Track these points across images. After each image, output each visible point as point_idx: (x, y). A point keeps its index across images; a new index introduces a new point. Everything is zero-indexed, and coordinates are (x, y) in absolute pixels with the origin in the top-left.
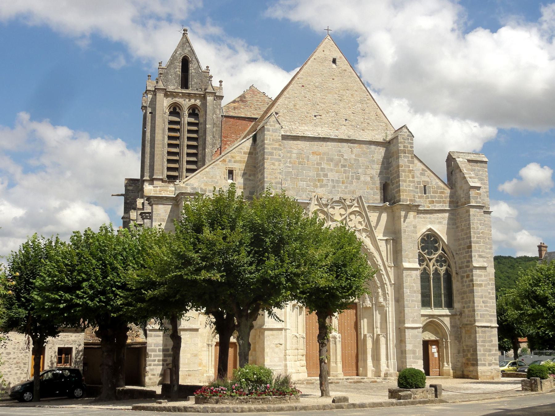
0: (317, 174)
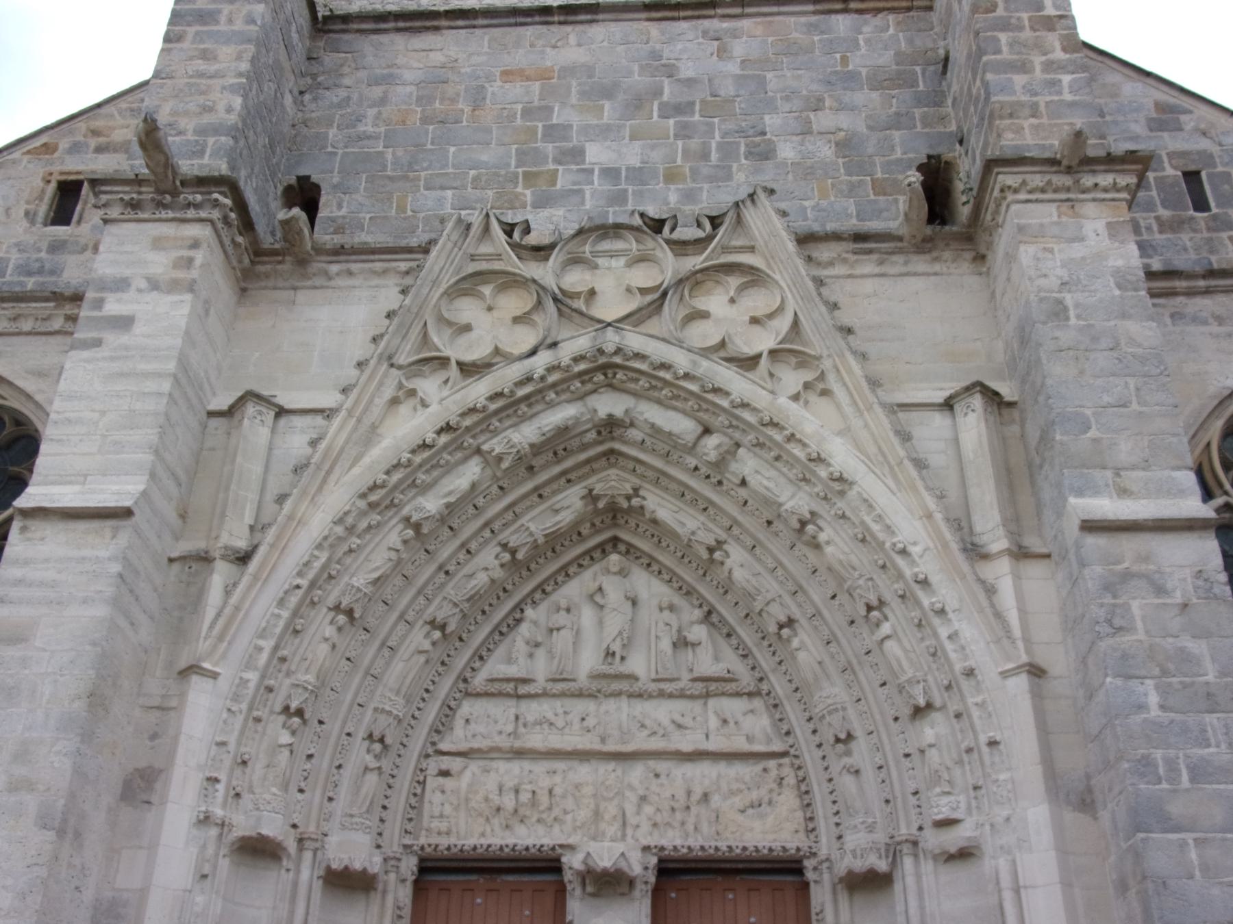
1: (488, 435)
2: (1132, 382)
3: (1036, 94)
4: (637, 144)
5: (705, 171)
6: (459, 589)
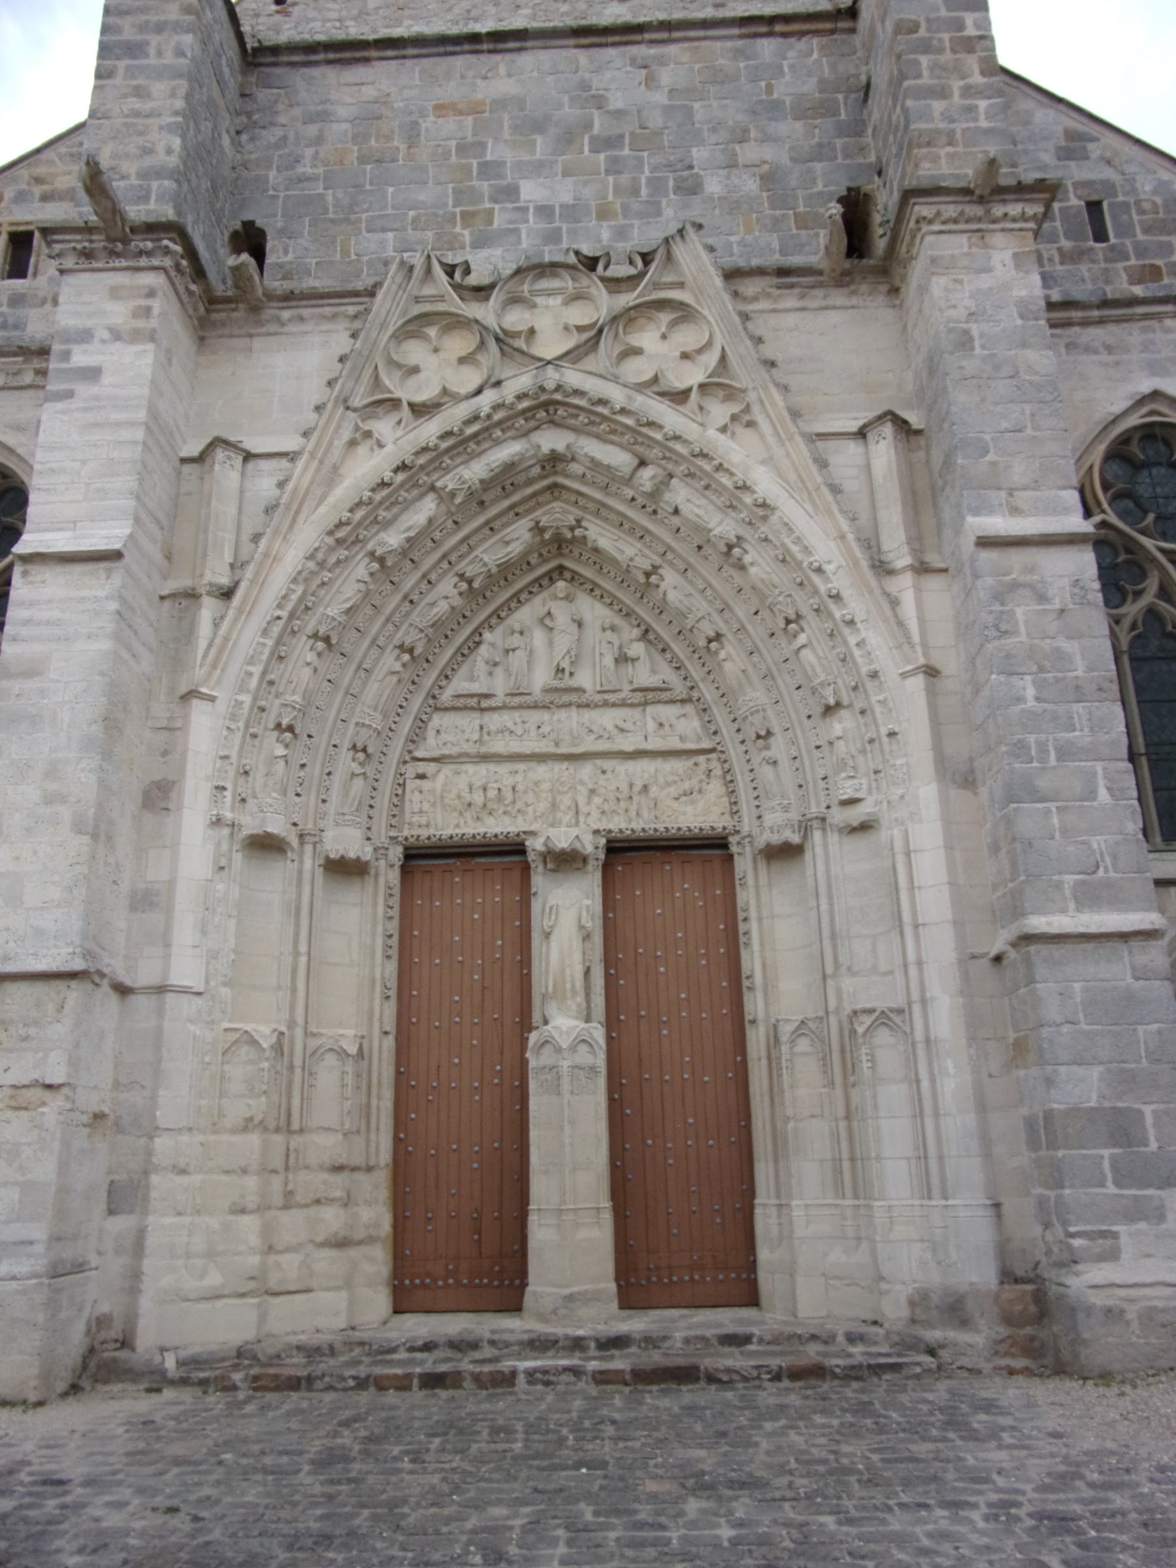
0: (457, 192)
1: (441, 473)
2: (1028, 408)
3: (952, 121)
4: (570, 179)
5: (636, 207)
6: (423, 616)
